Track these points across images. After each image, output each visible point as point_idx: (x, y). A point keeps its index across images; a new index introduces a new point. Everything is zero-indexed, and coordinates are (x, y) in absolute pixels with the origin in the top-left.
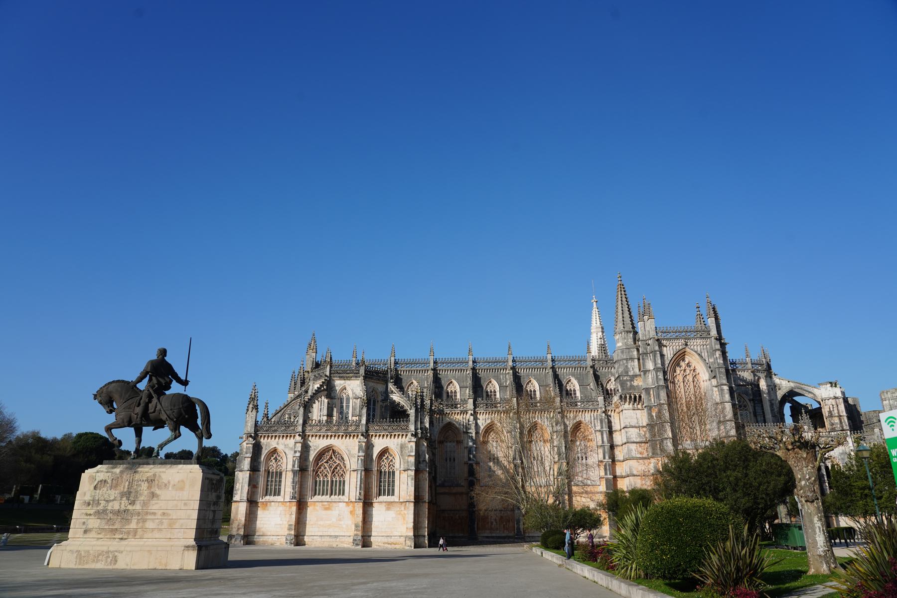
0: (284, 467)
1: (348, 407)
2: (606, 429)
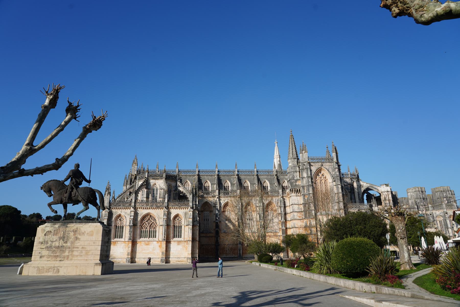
0: (125, 224)
1: (157, 193)
2: (283, 205)
